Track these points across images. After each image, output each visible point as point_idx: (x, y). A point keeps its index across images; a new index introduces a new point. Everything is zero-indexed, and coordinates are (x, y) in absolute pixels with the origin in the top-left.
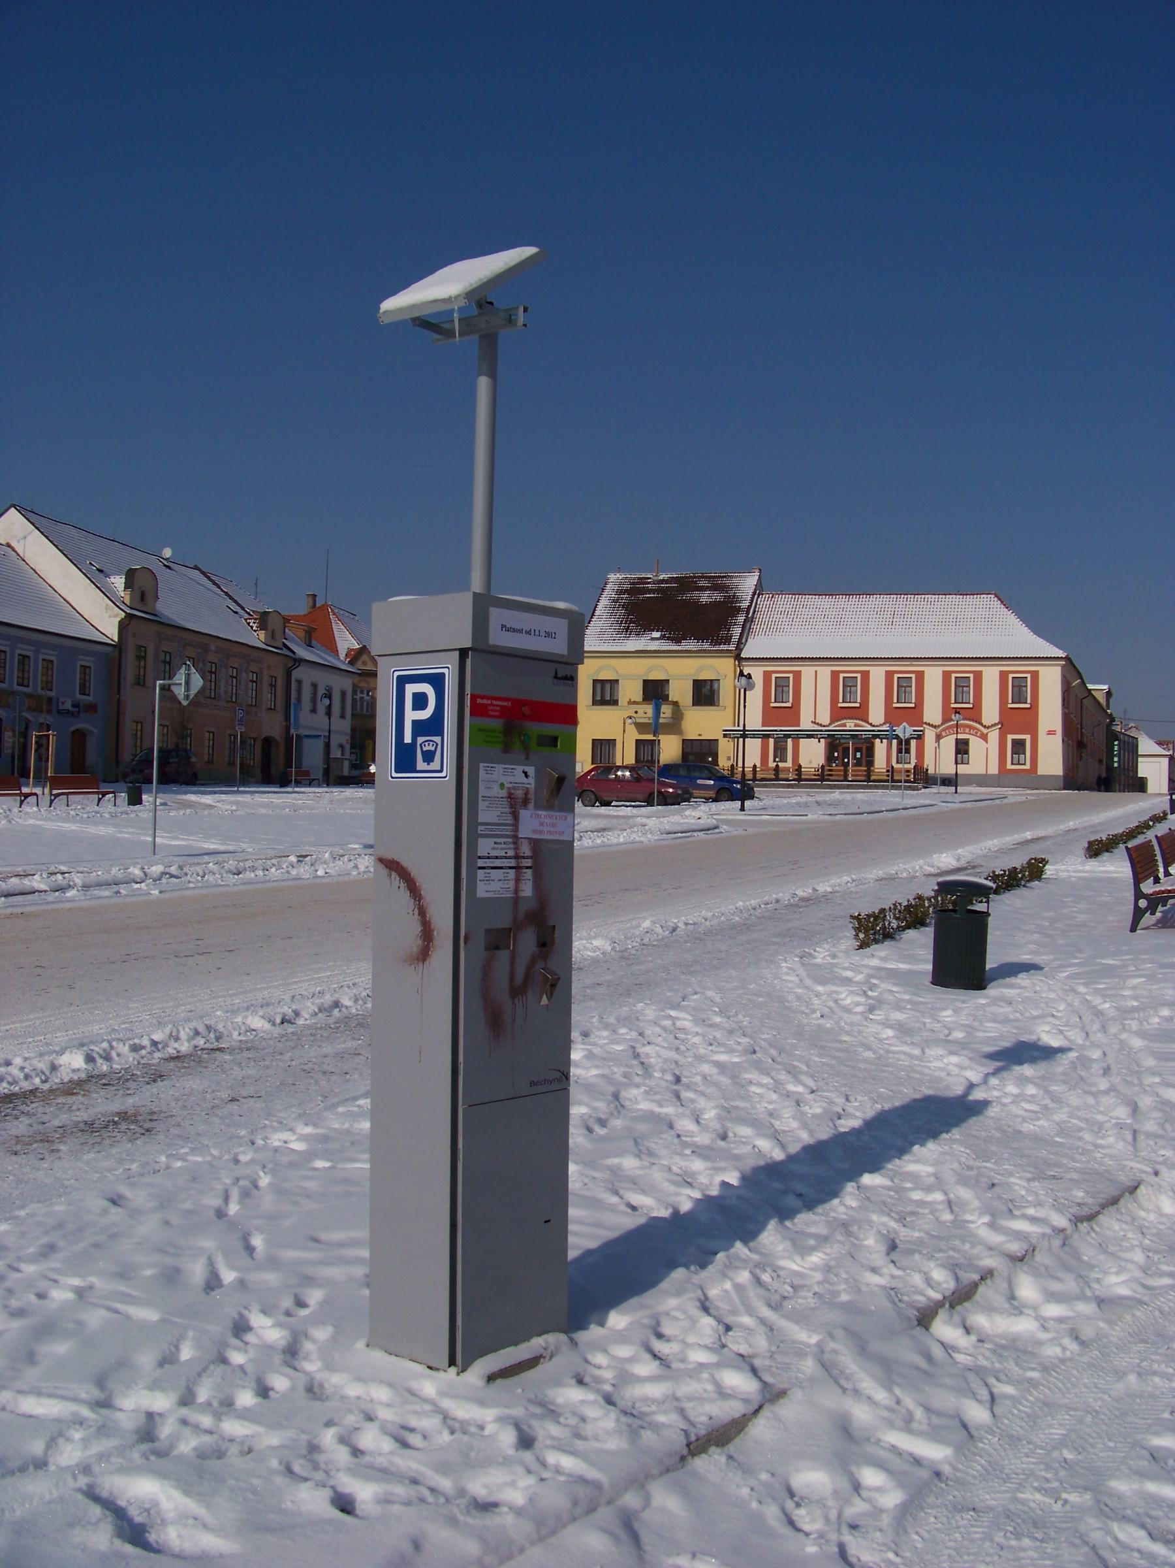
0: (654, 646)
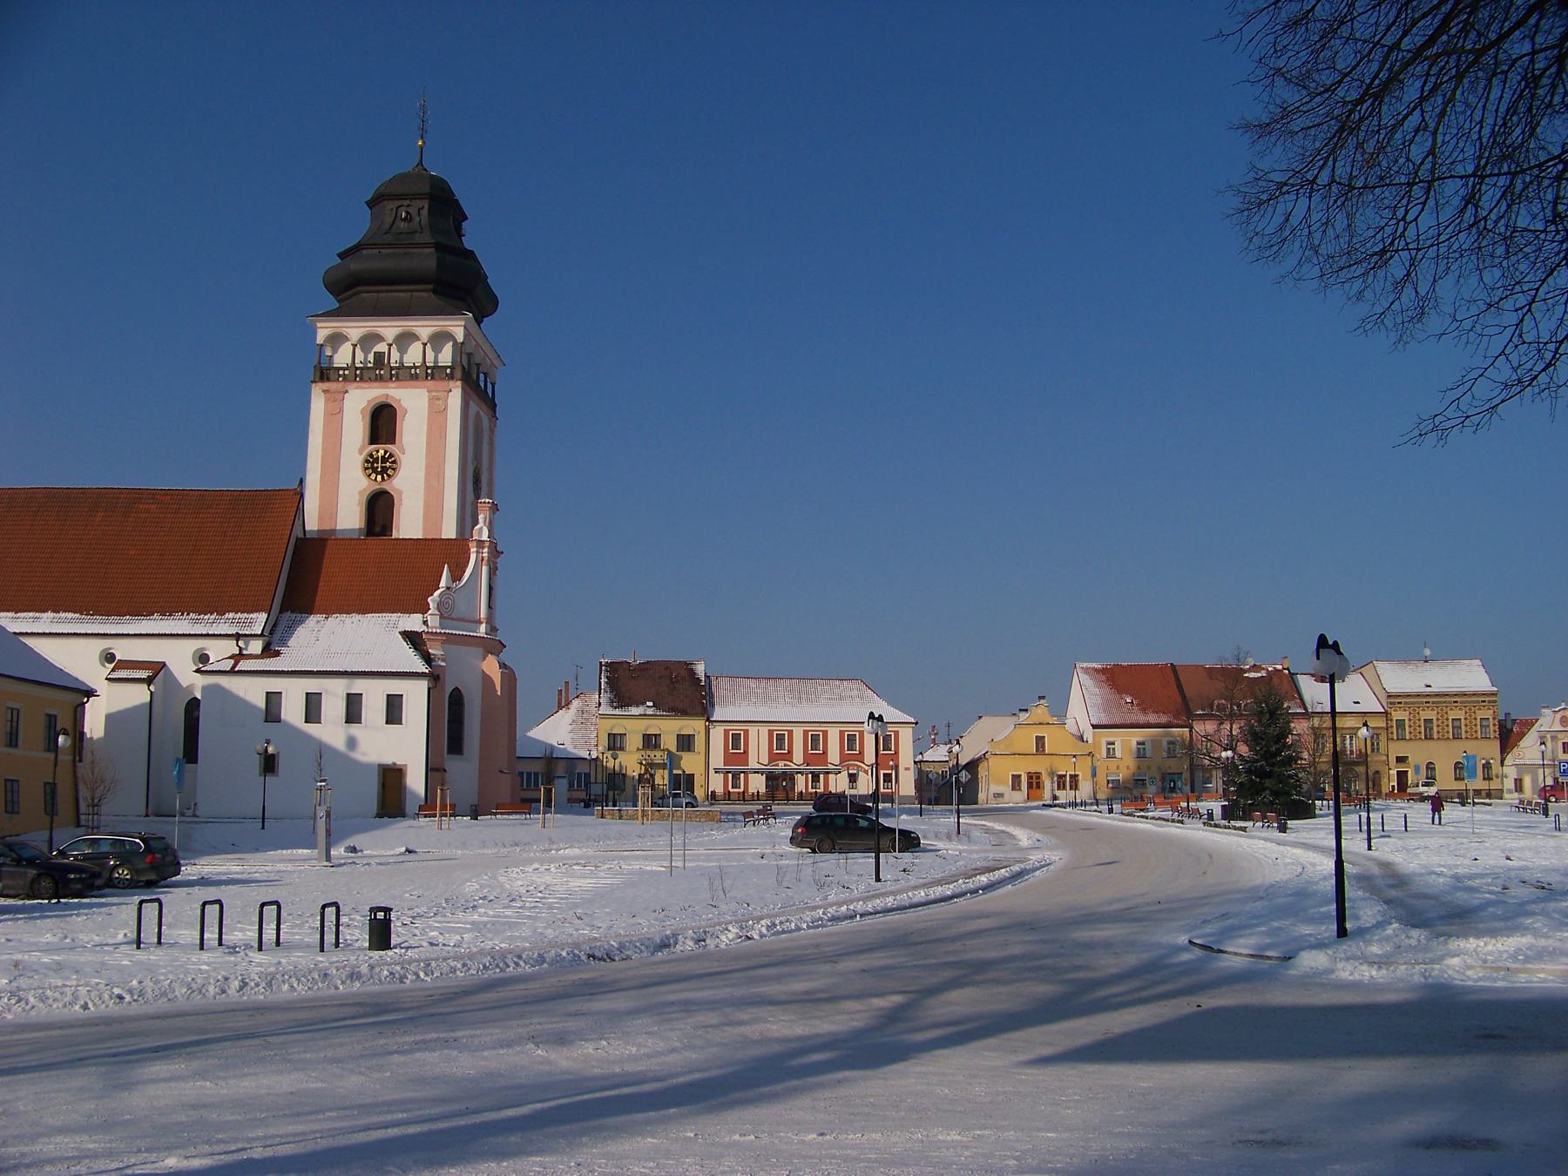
0: (650, 712)
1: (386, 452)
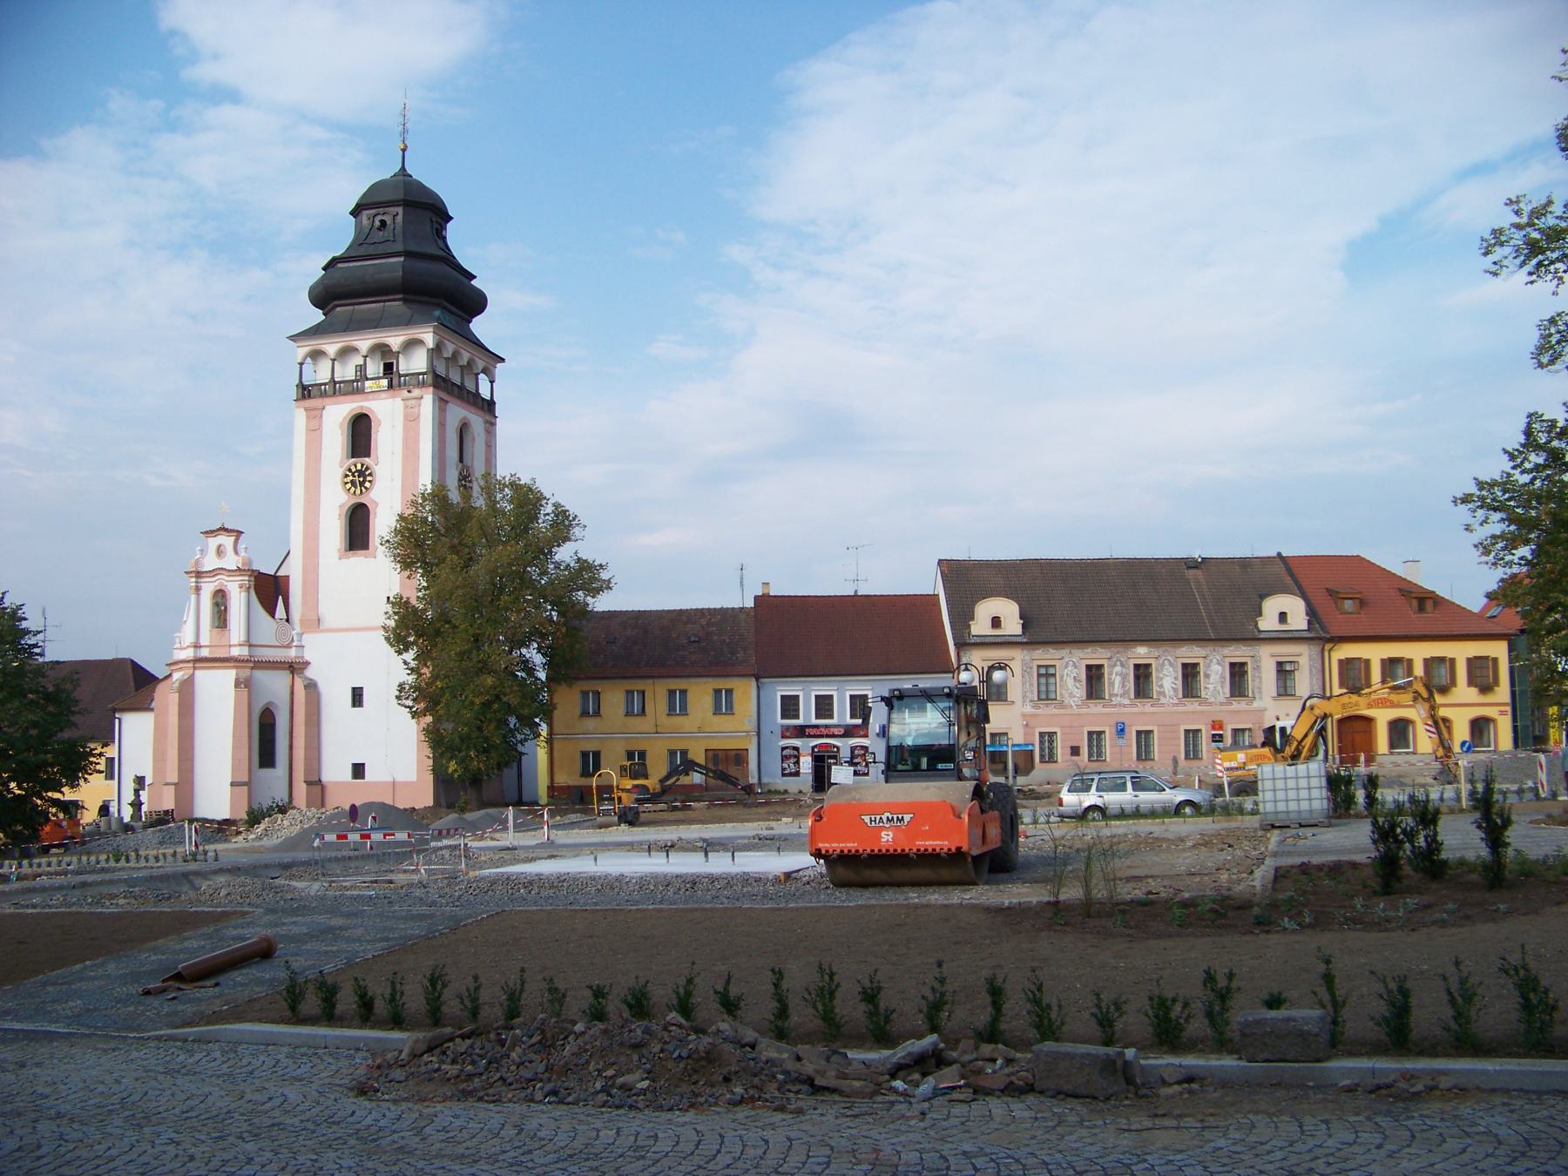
1: (362, 465)
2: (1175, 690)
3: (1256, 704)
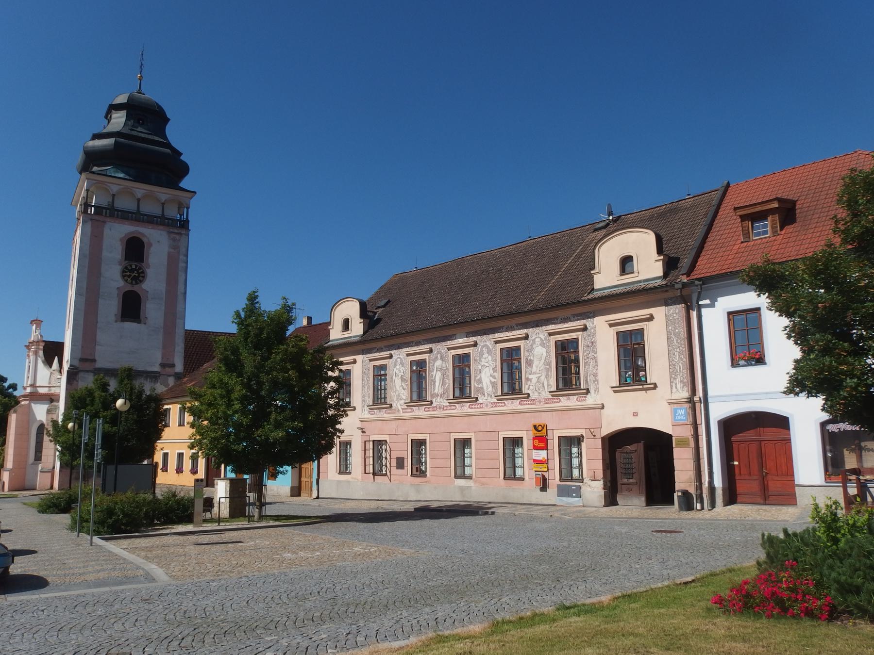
2: (494, 385)
3: (590, 400)
